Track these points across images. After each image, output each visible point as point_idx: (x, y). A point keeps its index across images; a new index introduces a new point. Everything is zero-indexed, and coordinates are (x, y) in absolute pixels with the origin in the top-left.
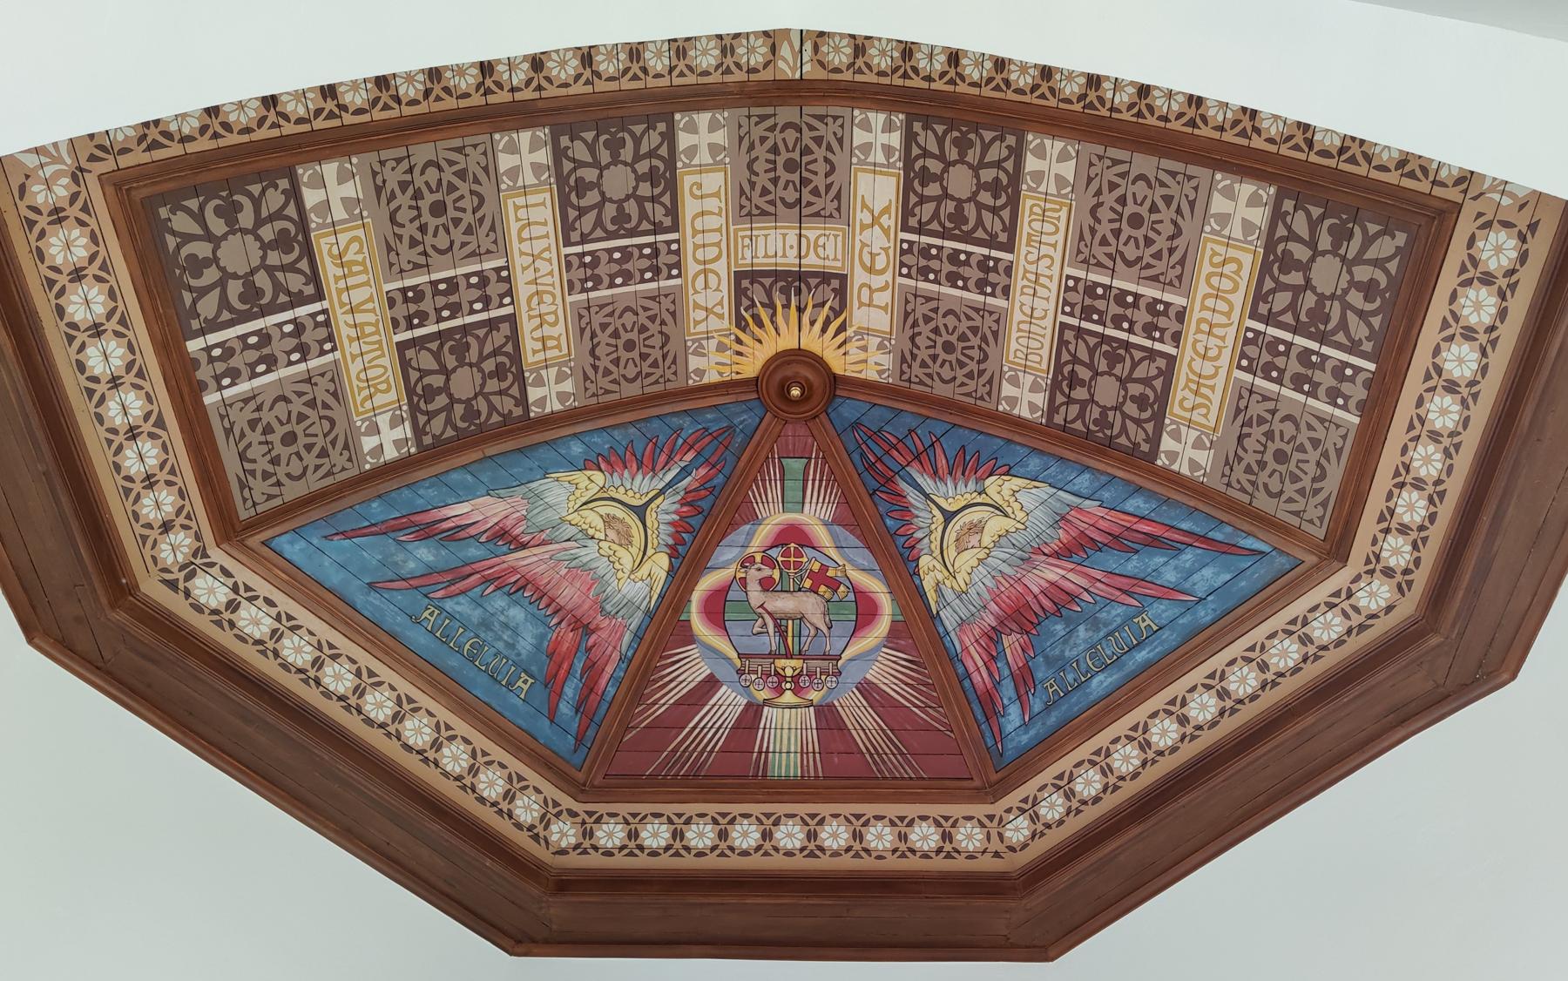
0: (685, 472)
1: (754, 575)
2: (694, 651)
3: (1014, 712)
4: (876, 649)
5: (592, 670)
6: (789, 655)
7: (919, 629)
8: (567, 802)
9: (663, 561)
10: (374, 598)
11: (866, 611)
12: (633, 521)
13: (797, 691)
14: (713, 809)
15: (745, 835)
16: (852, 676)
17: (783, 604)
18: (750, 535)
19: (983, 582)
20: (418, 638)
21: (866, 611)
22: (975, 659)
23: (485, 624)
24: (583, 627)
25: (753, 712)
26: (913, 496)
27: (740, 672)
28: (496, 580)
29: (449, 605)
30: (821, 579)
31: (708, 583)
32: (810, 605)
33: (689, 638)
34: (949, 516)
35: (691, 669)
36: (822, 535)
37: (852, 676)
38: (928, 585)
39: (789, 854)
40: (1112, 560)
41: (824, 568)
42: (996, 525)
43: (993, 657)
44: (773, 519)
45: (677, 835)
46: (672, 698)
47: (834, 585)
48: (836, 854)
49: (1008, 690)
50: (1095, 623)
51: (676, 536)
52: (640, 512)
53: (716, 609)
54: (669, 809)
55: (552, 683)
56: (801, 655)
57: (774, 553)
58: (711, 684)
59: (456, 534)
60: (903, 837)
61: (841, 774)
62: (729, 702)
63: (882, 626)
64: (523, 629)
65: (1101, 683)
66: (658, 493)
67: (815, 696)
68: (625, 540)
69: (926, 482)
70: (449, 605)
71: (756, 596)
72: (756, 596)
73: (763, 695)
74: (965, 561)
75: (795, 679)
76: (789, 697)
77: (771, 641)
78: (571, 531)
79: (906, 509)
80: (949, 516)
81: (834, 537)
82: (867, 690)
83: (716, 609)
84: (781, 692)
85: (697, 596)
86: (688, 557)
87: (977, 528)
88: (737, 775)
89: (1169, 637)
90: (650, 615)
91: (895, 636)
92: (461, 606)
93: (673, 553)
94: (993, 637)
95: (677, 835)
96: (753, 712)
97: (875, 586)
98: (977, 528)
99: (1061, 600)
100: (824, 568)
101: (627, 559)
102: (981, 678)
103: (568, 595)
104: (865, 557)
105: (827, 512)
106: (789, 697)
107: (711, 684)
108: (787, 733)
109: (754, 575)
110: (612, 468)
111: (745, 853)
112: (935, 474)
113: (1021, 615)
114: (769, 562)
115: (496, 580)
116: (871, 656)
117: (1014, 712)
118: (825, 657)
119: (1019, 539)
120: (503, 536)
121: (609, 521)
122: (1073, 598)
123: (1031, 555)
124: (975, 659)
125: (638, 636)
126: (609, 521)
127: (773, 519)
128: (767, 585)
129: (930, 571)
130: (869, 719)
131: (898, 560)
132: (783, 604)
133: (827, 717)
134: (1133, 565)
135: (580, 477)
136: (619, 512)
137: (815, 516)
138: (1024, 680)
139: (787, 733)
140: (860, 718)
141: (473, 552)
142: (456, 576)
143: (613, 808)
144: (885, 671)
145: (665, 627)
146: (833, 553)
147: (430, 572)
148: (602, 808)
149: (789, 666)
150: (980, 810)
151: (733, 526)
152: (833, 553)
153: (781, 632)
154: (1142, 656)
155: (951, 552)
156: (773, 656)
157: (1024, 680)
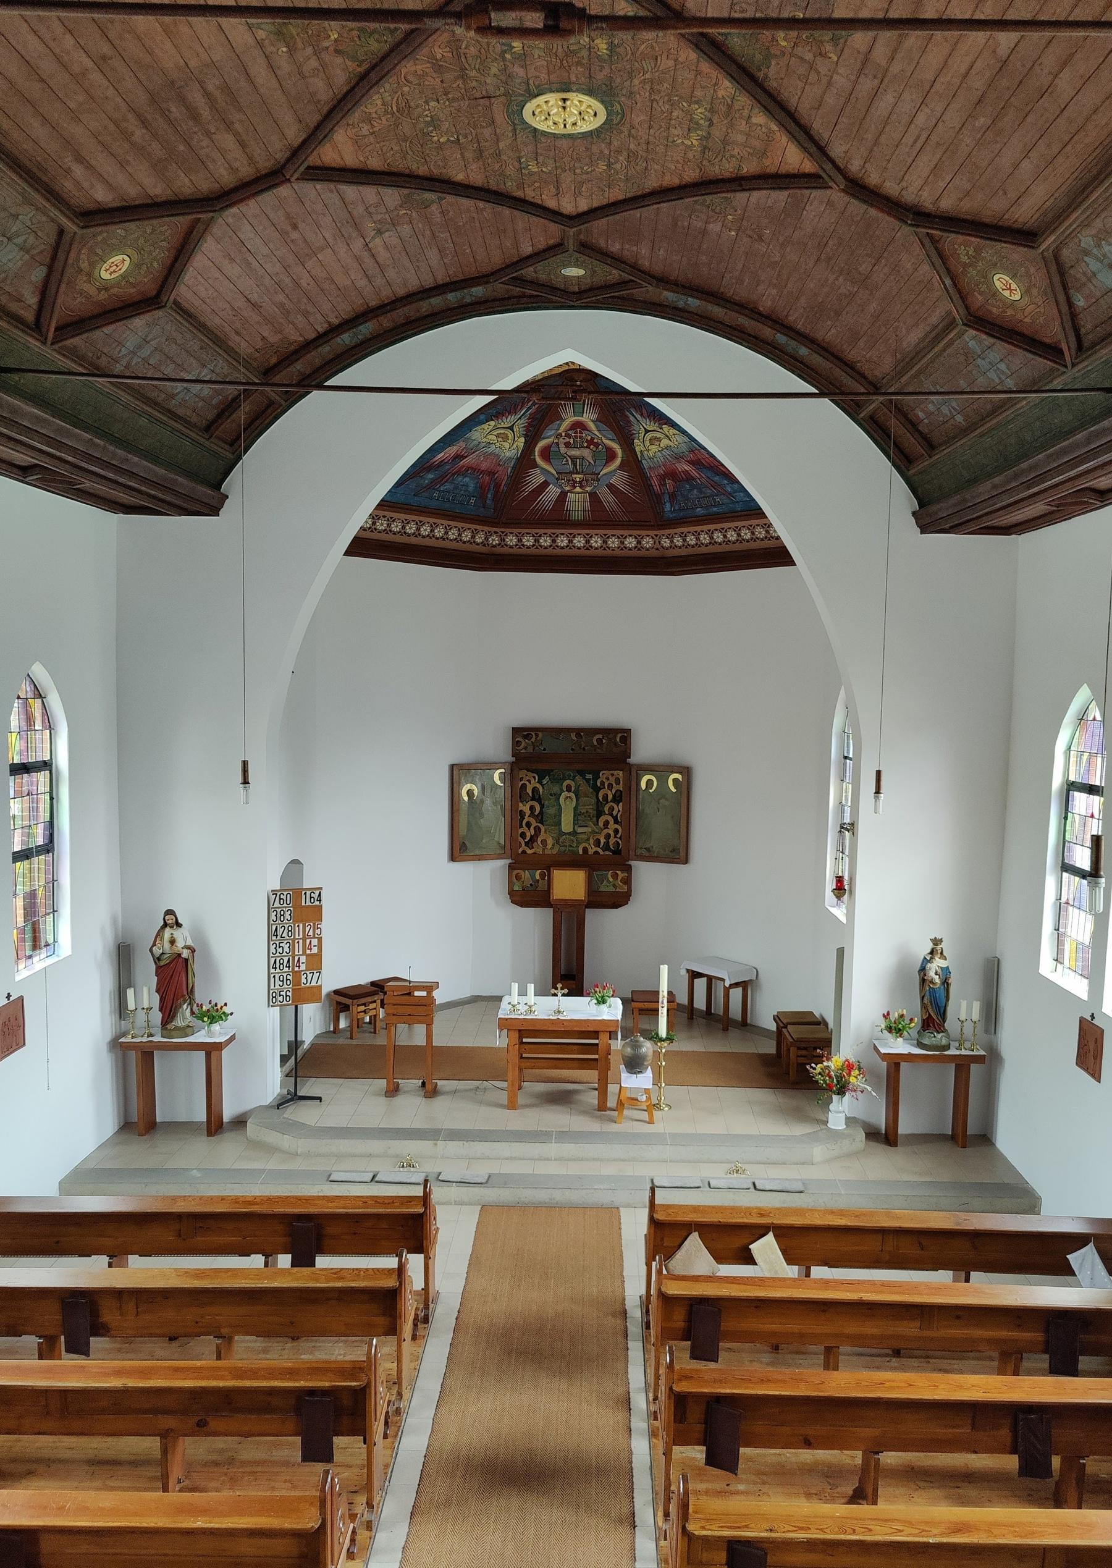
0: (529, 408)
3: (668, 505)
4: (615, 470)
5: (497, 486)
7: (633, 463)
9: (523, 440)
10: (417, 498)
11: (611, 455)
12: (509, 433)
15: (562, 541)
18: (559, 426)
20: (434, 504)
21: (611, 455)
23: (455, 488)
24: (491, 473)
25: (563, 495)
26: (632, 418)
27: (558, 479)
28: (458, 473)
30: (591, 442)
31: (542, 444)
32: (587, 453)
33: (536, 466)
34: (647, 431)
35: (536, 478)
36: (592, 426)
38: (637, 449)
39: (579, 548)
41: (592, 439)
42: (665, 442)
43: (662, 484)
44: (569, 419)
45: (537, 541)
47: (597, 445)
49: (666, 498)
50: (701, 492)
52: (511, 428)
53: (546, 454)
55: (482, 496)
58: (545, 484)
59: (441, 464)
61: (599, 518)
62: (553, 491)
63: (618, 462)
64: (469, 482)
66: (518, 421)
67: (588, 489)
69: (639, 417)
71: (563, 450)
72: (563, 450)
73: (567, 488)
74: (654, 449)
75: (580, 482)
76: (578, 489)
79: (630, 421)
80: (647, 431)
82: (610, 487)
83: (546, 454)
85: (537, 449)
86: (532, 435)
88: (558, 518)
89: (725, 509)
90: (518, 459)
91: (621, 467)
92: (447, 486)
93: (526, 436)
94: (662, 478)
95: (537, 541)
96: (563, 495)
97: (615, 446)
99: (689, 478)
100: (592, 439)
101: (507, 445)
102: (657, 488)
103: (484, 466)
104: (611, 435)
105: (594, 417)
106: (578, 489)
107: (545, 484)
108: (577, 502)
110: (497, 417)
111: (562, 548)
112: (642, 415)
113: (672, 474)
115: (458, 473)
116: (613, 473)
117: (668, 505)
118: (593, 473)
119: (676, 451)
120: (458, 457)
121: (498, 436)
122: (693, 479)
123: (678, 457)
124: (655, 482)
126: (498, 436)
127: (569, 419)
128: (567, 445)
130: (611, 498)
131: (626, 439)
133: (593, 496)
134: (716, 479)
135: (485, 426)
137: (588, 417)
139: (577, 502)
140: (608, 499)
142: (441, 479)
144: (619, 479)
145: (525, 461)
148: (507, 530)
149: (578, 477)
150: (652, 533)
153: (575, 465)
156: (571, 473)
157: (673, 497)
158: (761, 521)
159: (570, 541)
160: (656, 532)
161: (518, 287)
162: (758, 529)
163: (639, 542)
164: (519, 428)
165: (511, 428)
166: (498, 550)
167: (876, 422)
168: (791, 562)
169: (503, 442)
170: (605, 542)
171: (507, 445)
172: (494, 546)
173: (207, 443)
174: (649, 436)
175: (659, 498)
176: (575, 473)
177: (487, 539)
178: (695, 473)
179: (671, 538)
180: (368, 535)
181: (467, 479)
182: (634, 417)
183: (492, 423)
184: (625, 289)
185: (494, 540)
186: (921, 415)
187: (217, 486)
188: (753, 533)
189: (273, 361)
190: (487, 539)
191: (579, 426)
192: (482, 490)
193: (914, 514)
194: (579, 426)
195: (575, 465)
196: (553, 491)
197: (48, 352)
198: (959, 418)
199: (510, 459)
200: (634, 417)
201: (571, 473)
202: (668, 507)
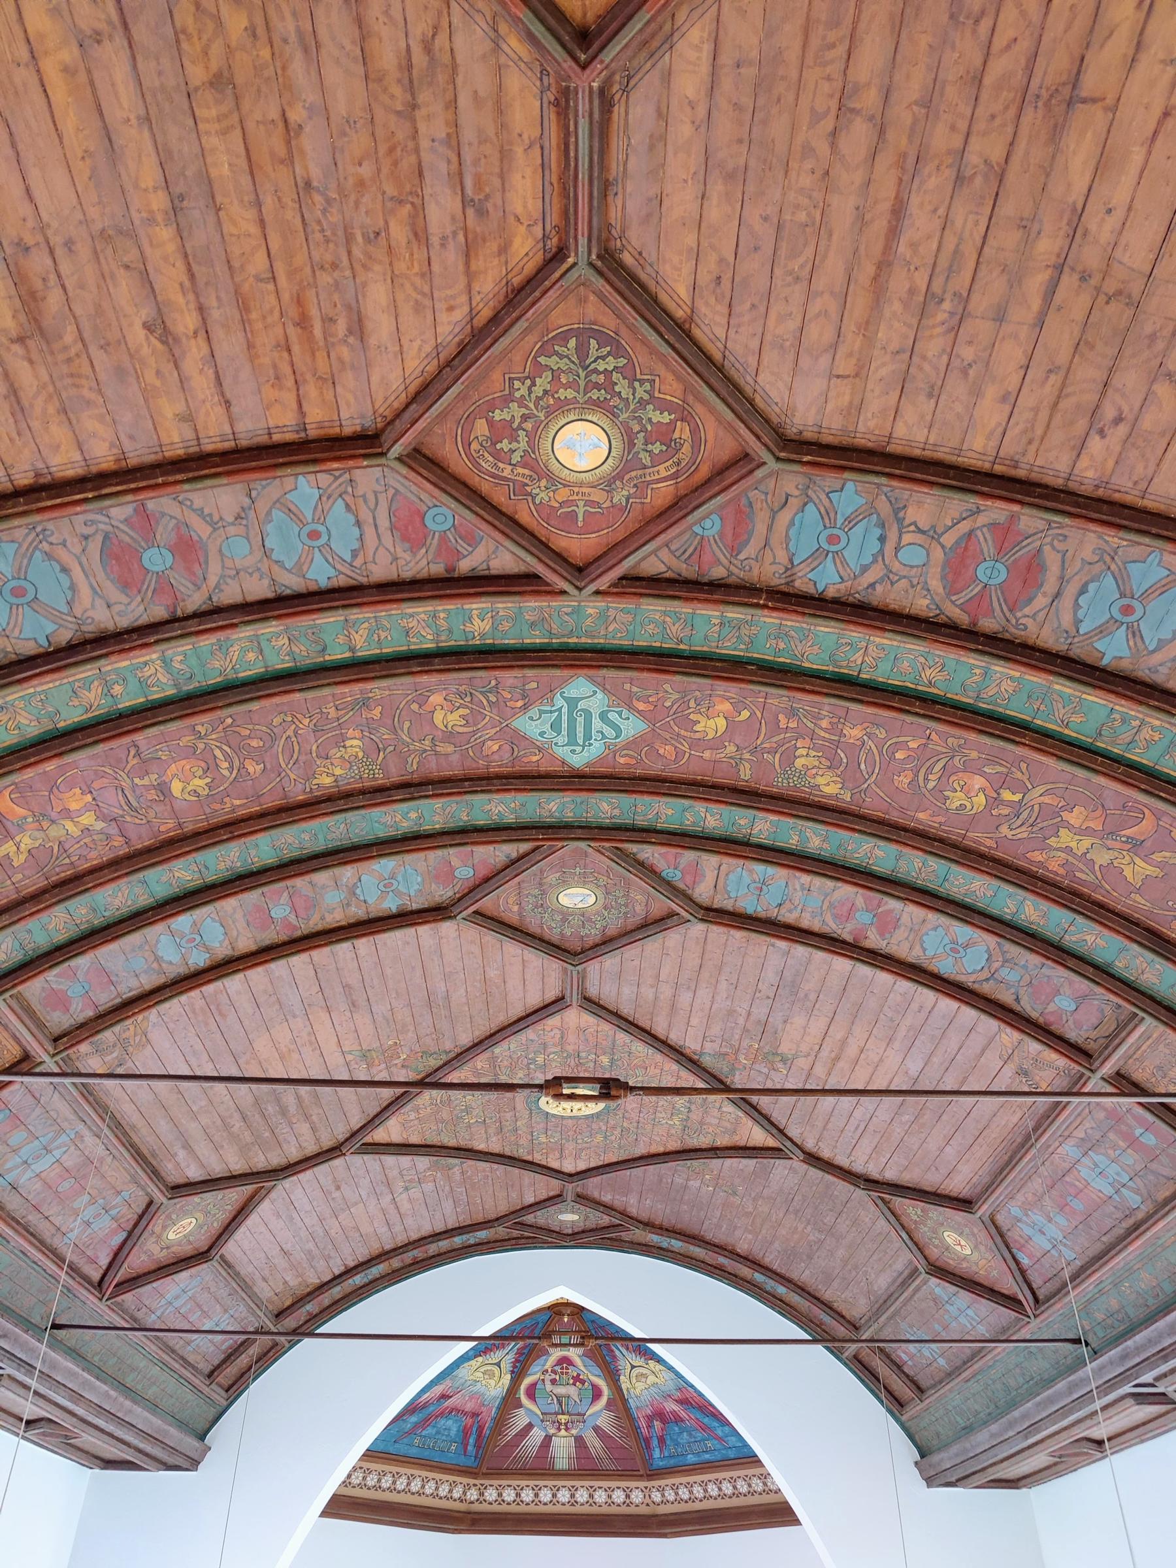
1: (548, 1378)
2: (522, 1411)
3: (657, 1450)
5: (481, 1429)
6: (563, 1414)
7: (619, 1403)
8: (472, 1481)
9: (509, 1376)
10: (397, 1445)
11: (597, 1394)
12: (496, 1369)
13: (567, 1429)
14: (532, 1483)
16: (590, 1423)
17: (560, 1390)
18: (546, 1361)
19: (646, 1397)
20: (413, 1452)
21: (597, 1394)
22: (643, 1423)
23: (438, 1433)
24: (475, 1415)
25: (548, 1439)
26: (617, 1353)
27: (542, 1421)
29: (424, 1433)
30: (577, 1379)
31: (527, 1381)
32: (572, 1391)
33: (520, 1405)
34: (633, 1367)
35: (520, 1419)
36: (578, 1361)
37: (590, 1423)
38: (624, 1387)
40: (699, 1415)
41: (579, 1375)
42: (651, 1379)
43: (650, 1426)
45: (518, 1495)
46: (514, 1432)
47: (583, 1382)
48: (582, 1505)
49: (655, 1442)
50: (690, 1435)
51: (515, 1367)
52: (498, 1364)
54: (514, 1483)
56: (569, 1414)
57: (558, 1368)
58: (530, 1426)
60: (610, 1497)
61: (586, 1468)
62: (537, 1435)
63: (604, 1401)
64: (452, 1426)
65: (691, 1458)
66: (506, 1356)
67: (574, 1432)
68: (492, 1376)
69: (624, 1351)
70: (424, 1433)
72: (549, 1387)
73: (552, 1431)
74: (640, 1386)
75: (566, 1424)
76: (563, 1432)
77: (556, 1407)
78: (469, 1383)
79: (614, 1357)
80: (633, 1367)
81: (583, 1361)
82: (596, 1429)
83: (531, 1393)
84: (559, 1429)
86: (518, 1373)
87: (645, 1376)
88: (541, 1468)
89: (717, 1456)
91: (609, 1406)
92: (430, 1431)
93: (512, 1372)
94: (650, 1419)
95: (518, 1495)
96: (548, 1439)
97: (601, 1383)
98: (645, 1376)
99: (678, 1419)
100: (579, 1375)
101: (492, 1382)
102: (645, 1431)
103: (469, 1407)
104: (598, 1371)
106: (563, 1432)
107: (530, 1426)
109: (548, 1378)
110: (485, 1353)
112: (627, 1349)
113: (659, 1415)
114: (555, 1372)
116: (599, 1414)
118: (579, 1414)
119: (663, 1388)
120: (444, 1397)
122: (682, 1421)
124: (643, 1423)
125: (498, 1408)
128: (553, 1382)
129: (625, 1383)
131: (613, 1376)
132: (560, 1390)
133: (579, 1440)
134: (706, 1420)
135: (473, 1362)
136: (489, 1367)
138: (662, 1440)
140: (594, 1443)
141: (432, 1409)
143: (491, 1482)
145: (510, 1401)
146: (582, 1368)
147: (416, 1426)
148: (487, 1482)
149: (563, 1418)
150: (642, 1484)
151: (539, 1357)
152: (582, 1368)
153: (560, 1404)
154: (707, 1456)
155: (634, 1380)
156: (556, 1414)
157: (662, 1440)
158: (757, 1471)
159: (554, 1496)
160: (646, 1484)
161: (519, 1231)
162: (755, 1481)
163: (628, 1496)
164: (506, 1365)
165: (498, 1364)
166: (477, 1507)
167: (860, 1362)
168: (796, 1522)
169: (489, 1382)
170: (591, 1496)
171: (492, 1382)
172: (472, 1503)
173: (206, 1390)
174: (635, 1372)
175: (647, 1441)
176: (562, 1415)
177: (465, 1493)
178: (683, 1414)
179: (661, 1490)
180: (349, 1492)
181: (450, 1422)
182: (619, 1349)
183: (480, 1359)
184: (613, 1232)
185: (473, 1495)
186: (904, 1356)
187: (202, 1437)
188: (750, 1486)
189: (288, 1303)
190: (465, 1493)
191: (565, 1361)
192: (466, 1432)
193: (916, 1463)
194: (565, 1361)
195: (560, 1404)
196: (537, 1435)
197: (102, 1307)
198: (942, 1361)
199: (495, 1398)
200: (619, 1349)
201: (556, 1414)
202: (657, 1453)
